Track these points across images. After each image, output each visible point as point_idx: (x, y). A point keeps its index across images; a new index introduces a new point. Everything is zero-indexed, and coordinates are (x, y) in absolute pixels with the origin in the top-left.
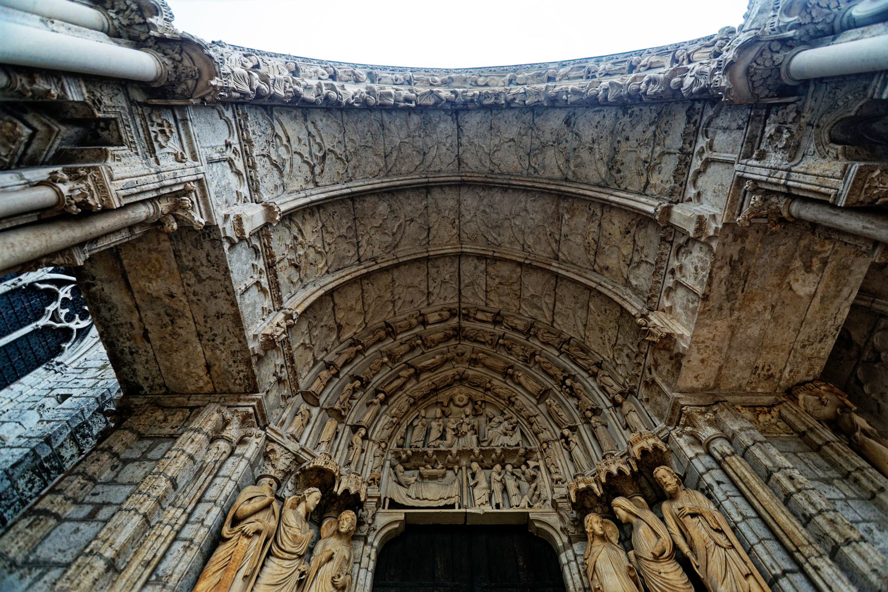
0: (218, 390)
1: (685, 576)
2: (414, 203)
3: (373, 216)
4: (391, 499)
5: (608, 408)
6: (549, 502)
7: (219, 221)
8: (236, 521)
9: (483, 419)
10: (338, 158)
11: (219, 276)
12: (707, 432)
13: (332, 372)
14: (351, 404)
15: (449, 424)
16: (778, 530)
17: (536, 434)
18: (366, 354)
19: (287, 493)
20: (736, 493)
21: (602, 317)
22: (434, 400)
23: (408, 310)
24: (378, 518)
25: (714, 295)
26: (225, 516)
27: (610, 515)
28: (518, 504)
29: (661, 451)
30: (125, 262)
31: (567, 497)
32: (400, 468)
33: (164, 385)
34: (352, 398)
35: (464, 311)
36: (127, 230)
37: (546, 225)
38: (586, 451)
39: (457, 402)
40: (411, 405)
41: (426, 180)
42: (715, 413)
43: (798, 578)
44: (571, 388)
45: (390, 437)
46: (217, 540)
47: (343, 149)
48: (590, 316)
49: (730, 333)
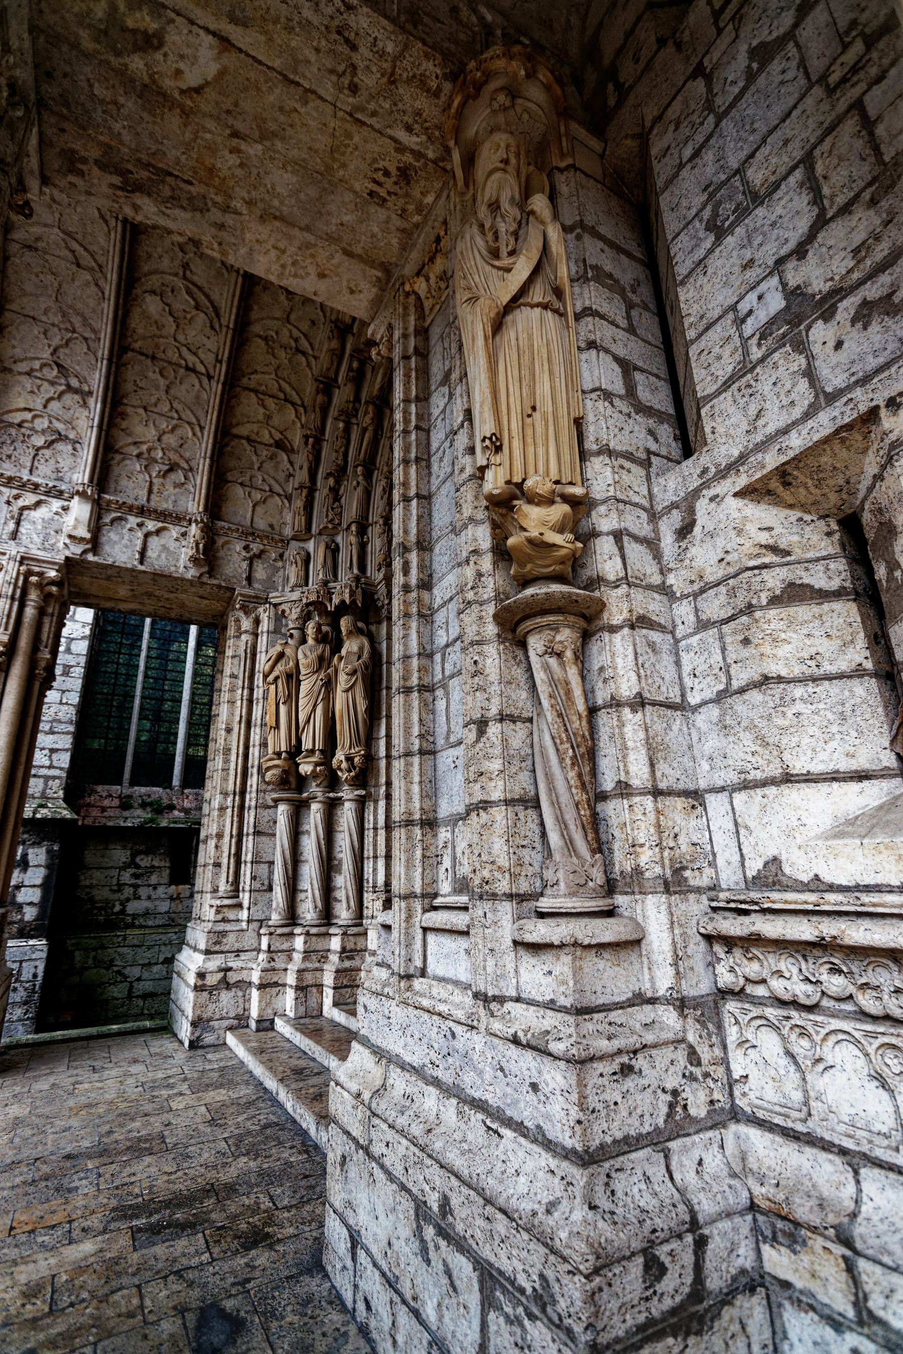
2: (159, 249)
10: (67, 344)
47: (56, 330)
49: (277, 224)
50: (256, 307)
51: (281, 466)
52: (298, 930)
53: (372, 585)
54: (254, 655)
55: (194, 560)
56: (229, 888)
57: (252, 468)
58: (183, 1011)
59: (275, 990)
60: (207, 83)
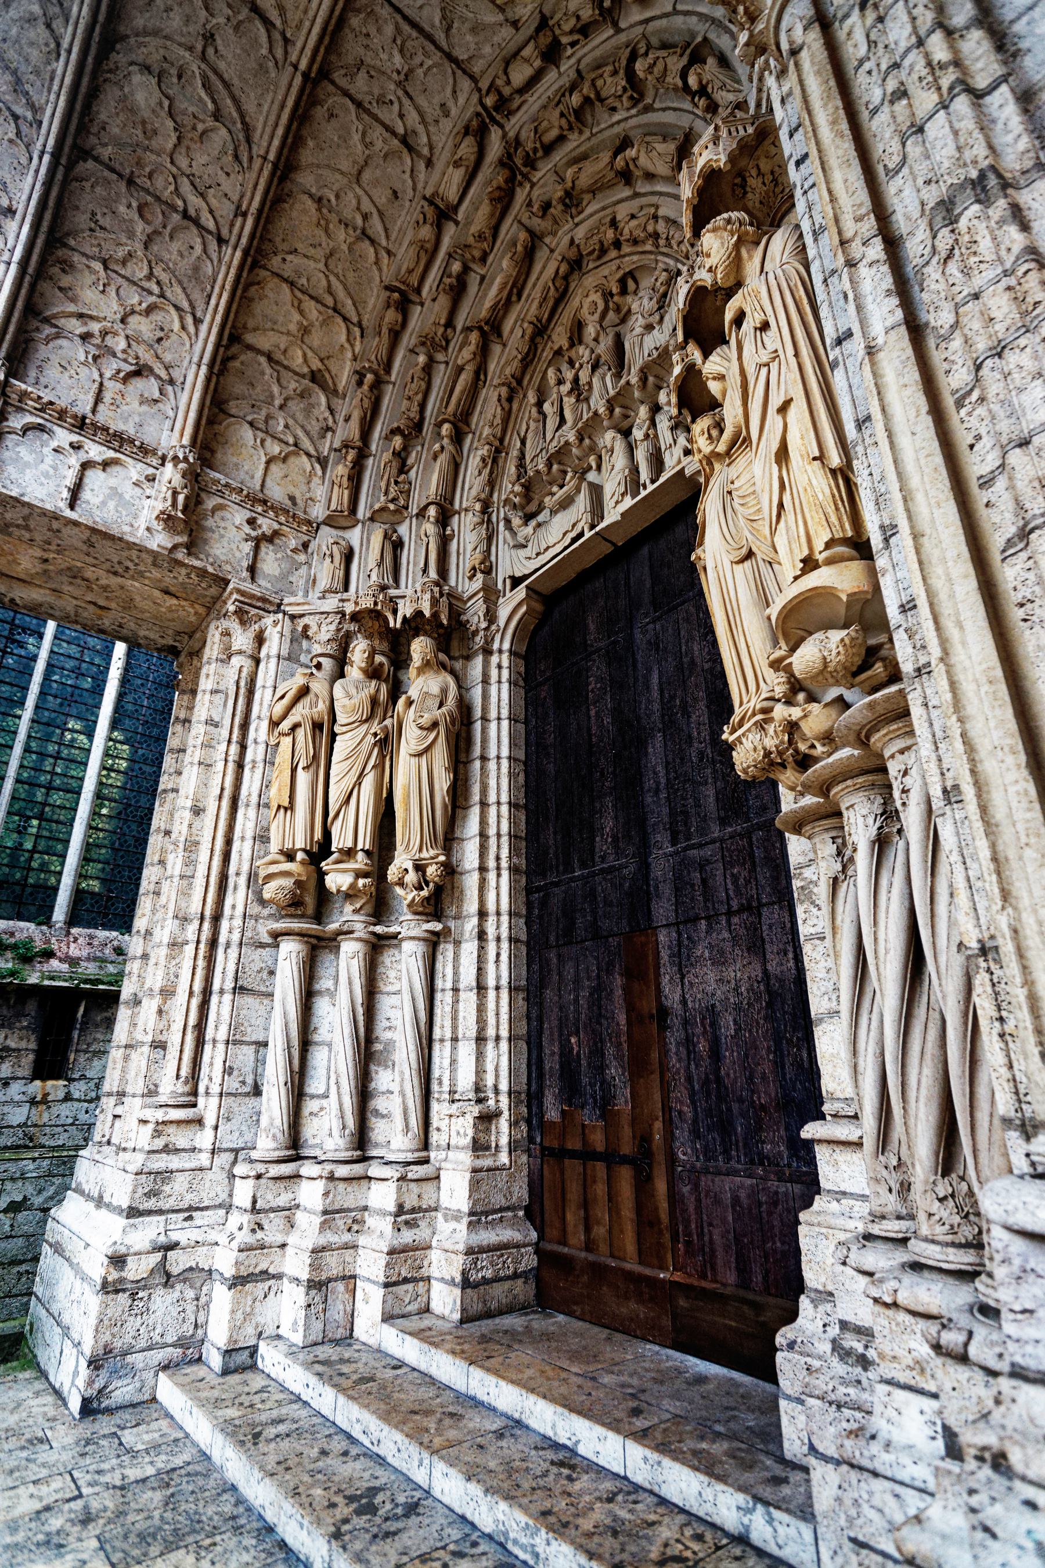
50: (311, 143)
51: (316, 412)
52: (308, 1169)
53: (459, 599)
54: (251, 692)
55: (167, 520)
56: (181, 1088)
57: (271, 404)
58: (66, 1331)
59: (262, 1287)
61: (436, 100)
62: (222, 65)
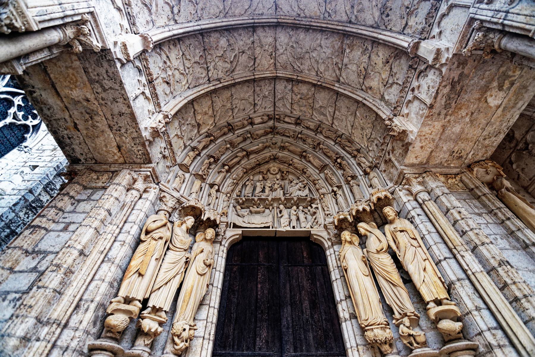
0: (127, 162)
1: (392, 260)
2: (244, 39)
3: (217, 48)
4: (234, 223)
5: (361, 176)
6: (322, 226)
7: (110, 46)
8: (147, 232)
9: (287, 182)
11: (117, 87)
12: (416, 188)
13: (196, 153)
14: (208, 172)
15: (267, 184)
16: (446, 238)
17: (318, 190)
18: (217, 143)
19: (175, 219)
20: (428, 221)
21: (364, 120)
22: (258, 170)
23: (242, 115)
24: (227, 232)
25: (437, 105)
26: (141, 230)
27: (356, 232)
28: (305, 226)
29: (389, 199)
30: (52, 76)
31: (333, 223)
32: (238, 207)
33: (94, 159)
34: (209, 168)
35: (277, 117)
36: (47, 49)
37: (333, 57)
38: (346, 199)
39: (272, 172)
40: (244, 173)
41: (253, 21)
42: (423, 178)
43: (452, 261)
44: (340, 164)
45: (232, 191)
46: (139, 242)
48: (356, 120)
50: (240, 86)
60: (488, 104)
61: (266, 105)
62: (240, 58)
